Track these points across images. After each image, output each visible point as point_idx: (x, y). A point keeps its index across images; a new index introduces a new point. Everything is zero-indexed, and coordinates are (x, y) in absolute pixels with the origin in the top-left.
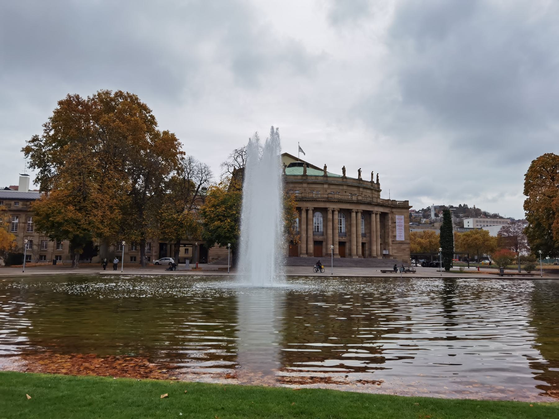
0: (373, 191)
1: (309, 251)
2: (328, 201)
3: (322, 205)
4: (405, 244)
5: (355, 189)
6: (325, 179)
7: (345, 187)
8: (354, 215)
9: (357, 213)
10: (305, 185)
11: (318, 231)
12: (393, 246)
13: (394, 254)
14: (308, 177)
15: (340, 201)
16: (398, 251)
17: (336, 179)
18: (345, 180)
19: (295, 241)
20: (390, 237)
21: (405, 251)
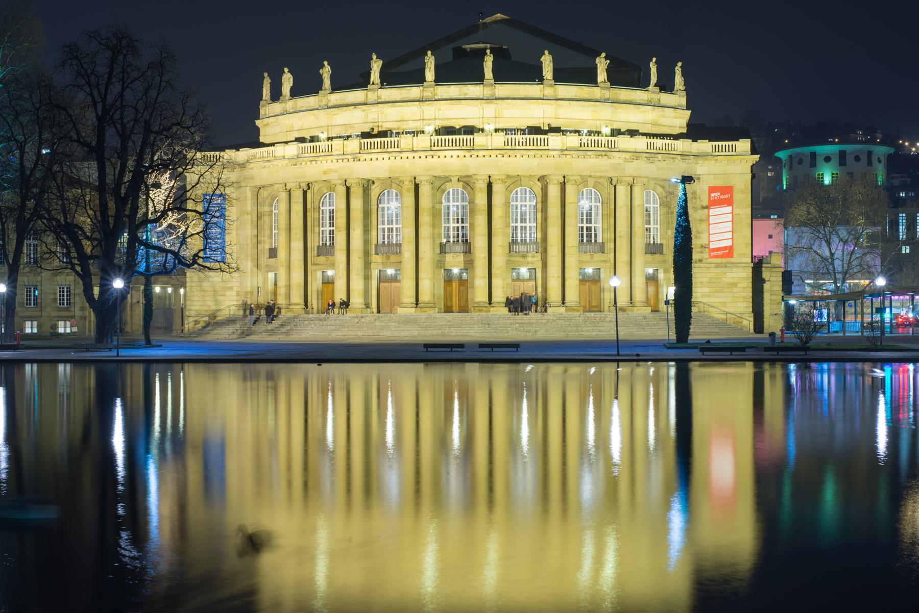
1: (421, 299)
21: (735, 290)
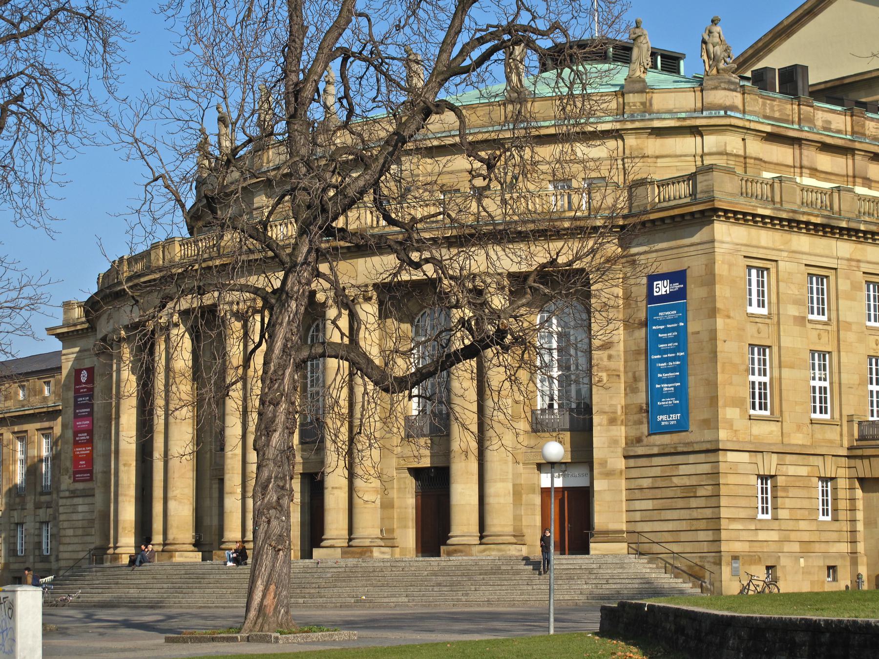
4: (692, 458)
12: (634, 473)
13: (641, 527)
16: (658, 504)
20: (596, 419)
21: (694, 503)
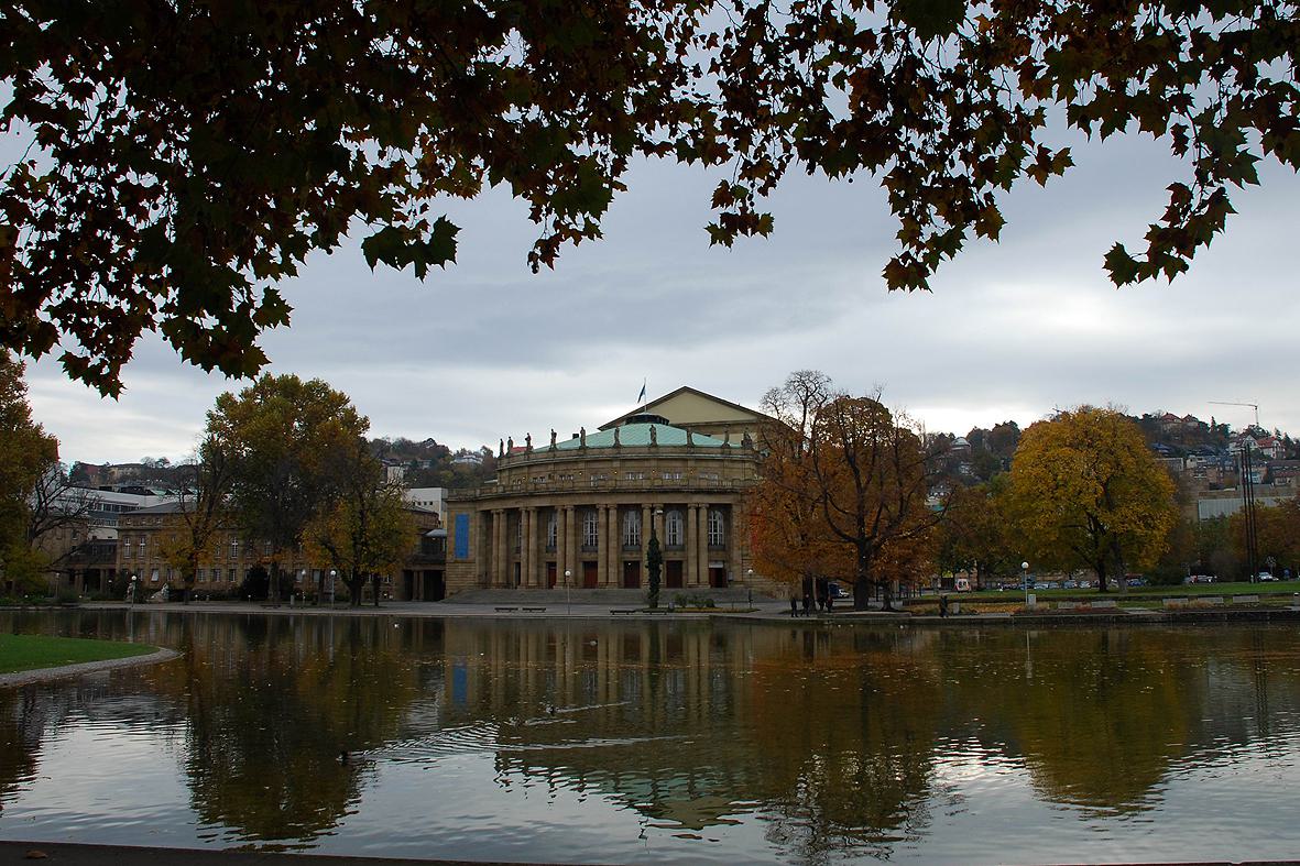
0: (726, 463)
2: (595, 493)
3: (586, 501)
5: (678, 464)
6: (615, 451)
7: (653, 463)
8: (646, 513)
9: (652, 510)
10: (581, 465)
11: (675, 544)
14: (588, 451)
15: (614, 492)
17: (638, 450)
18: (653, 450)
19: (269, 568)
